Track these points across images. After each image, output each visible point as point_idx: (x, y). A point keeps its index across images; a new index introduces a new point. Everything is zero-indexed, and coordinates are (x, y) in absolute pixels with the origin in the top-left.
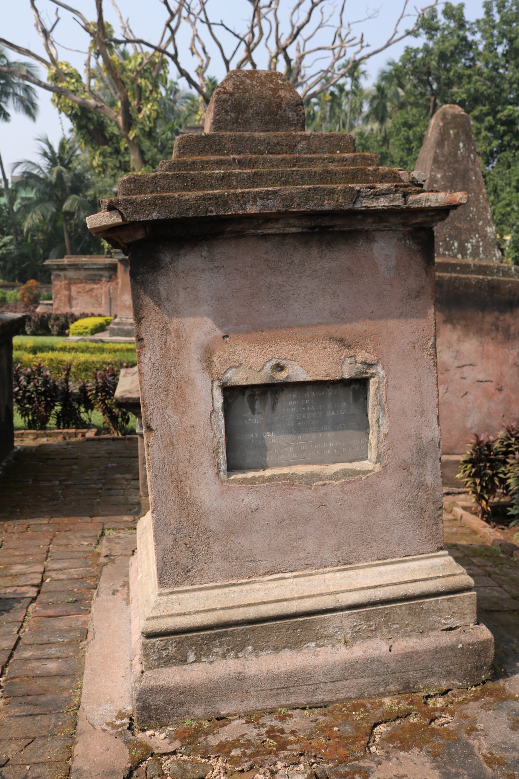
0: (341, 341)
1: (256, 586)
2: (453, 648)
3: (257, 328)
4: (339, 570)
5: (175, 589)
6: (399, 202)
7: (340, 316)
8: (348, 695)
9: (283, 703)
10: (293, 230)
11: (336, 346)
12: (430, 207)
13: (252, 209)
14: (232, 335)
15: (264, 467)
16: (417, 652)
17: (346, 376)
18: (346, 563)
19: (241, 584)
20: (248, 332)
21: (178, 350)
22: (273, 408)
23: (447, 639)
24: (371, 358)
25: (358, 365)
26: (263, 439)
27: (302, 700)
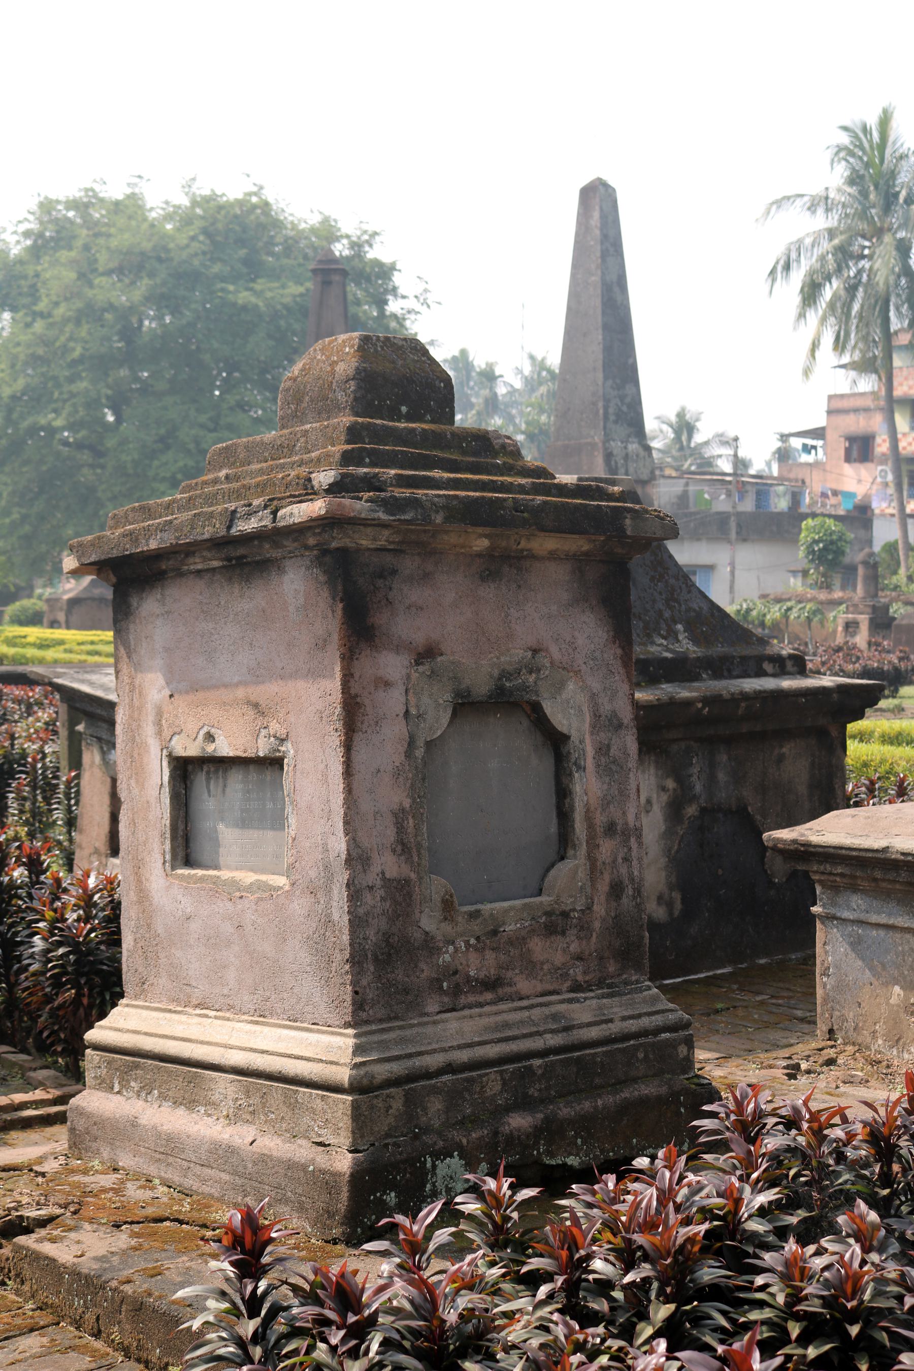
0: (256, 706)
1: (183, 1018)
2: (304, 1168)
3: (194, 688)
4: (252, 1022)
5: (134, 1003)
6: (267, 522)
7: (257, 676)
8: (213, 1191)
9: (163, 1174)
10: (216, 564)
11: (251, 713)
12: (294, 524)
13: (153, 545)
14: (176, 696)
15: (217, 867)
16: (270, 1157)
17: (261, 754)
18: (261, 1015)
19: (175, 1012)
20: (187, 692)
21: (140, 709)
22: (224, 791)
23: (302, 1151)
24: (282, 733)
25: (272, 739)
26: (216, 831)
27: (176, 1179)
